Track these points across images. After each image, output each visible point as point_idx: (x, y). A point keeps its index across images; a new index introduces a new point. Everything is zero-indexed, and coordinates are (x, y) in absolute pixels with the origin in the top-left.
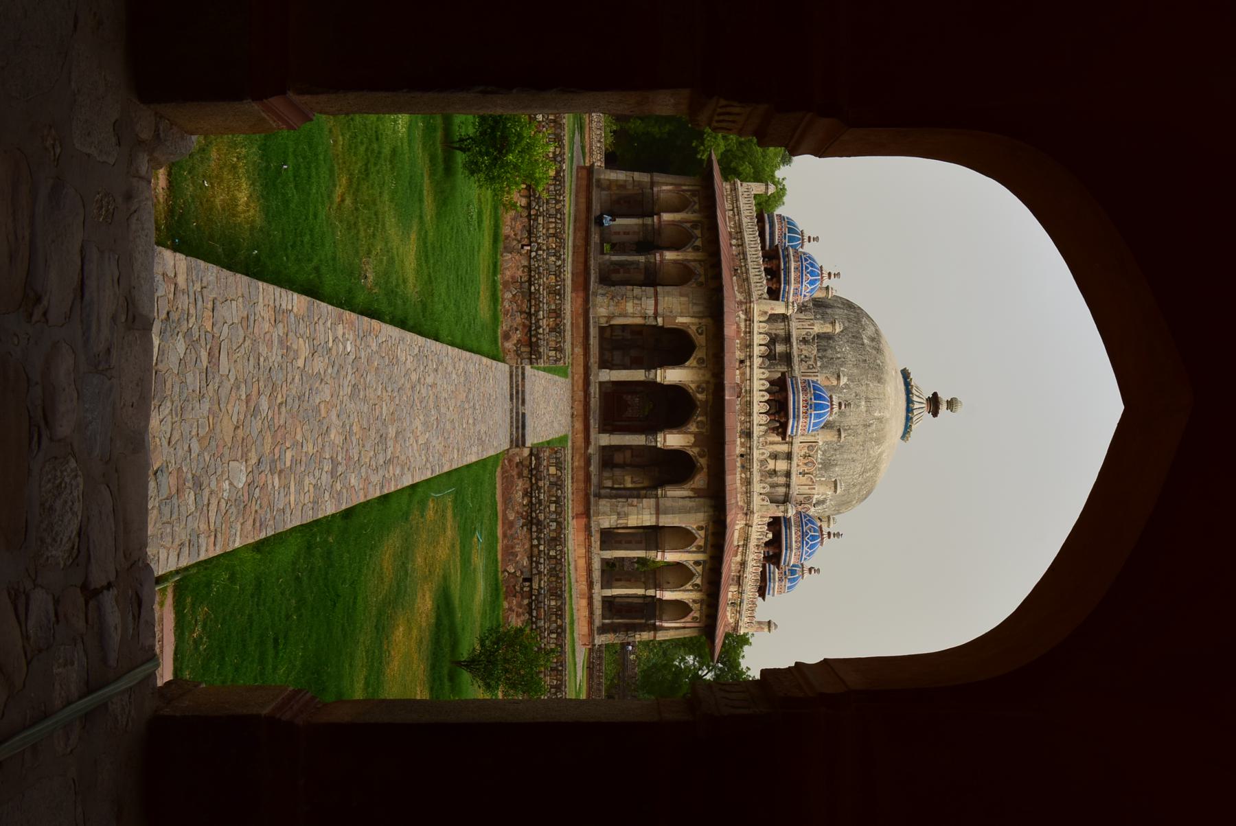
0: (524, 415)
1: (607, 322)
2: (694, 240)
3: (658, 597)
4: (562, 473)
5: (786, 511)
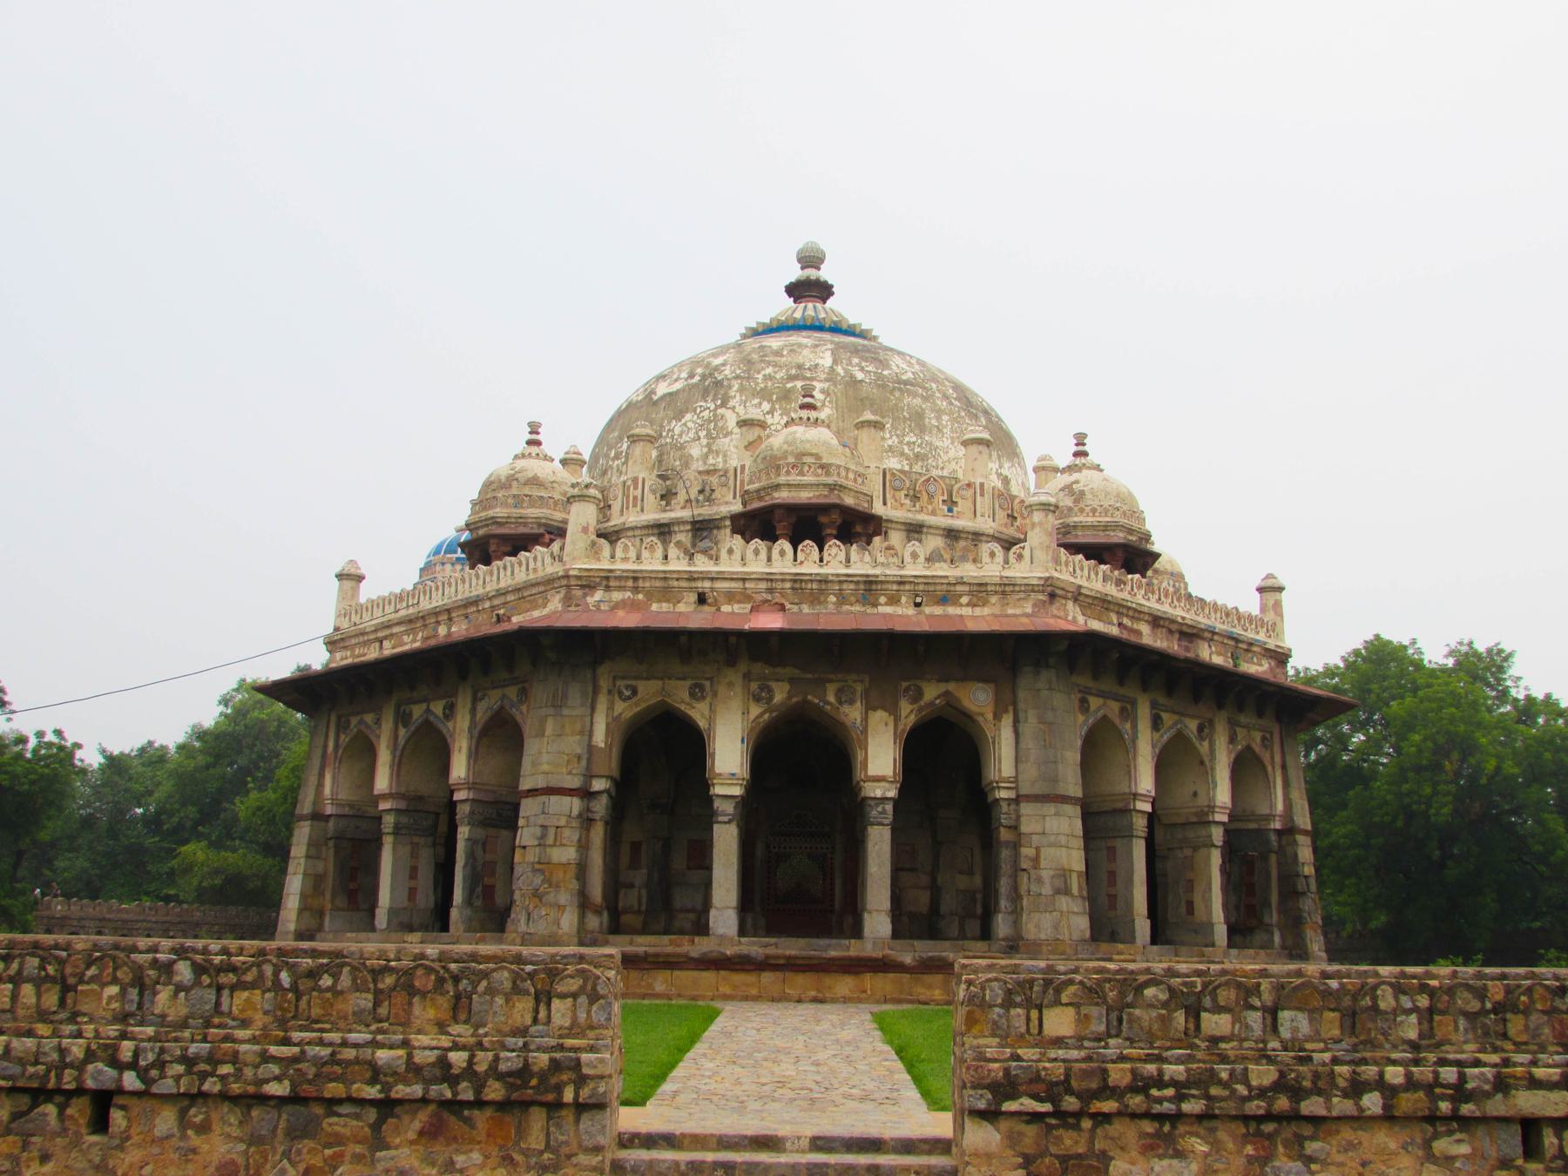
0: (820, 1143)
1: (598, 912)
2: (432, 718)
3: (1225, 819)
4: (1071, 982)
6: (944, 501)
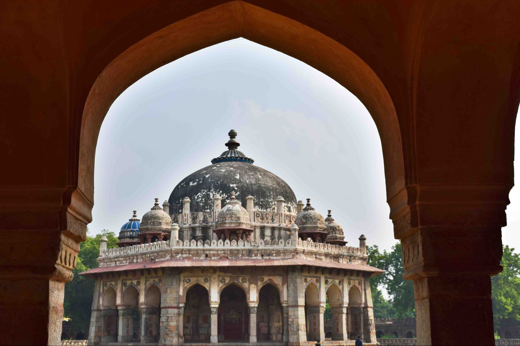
1: (182, 338)
2: (133, 285)
3: (347, 306)
5: (295, 230)
6: (271, 219)
